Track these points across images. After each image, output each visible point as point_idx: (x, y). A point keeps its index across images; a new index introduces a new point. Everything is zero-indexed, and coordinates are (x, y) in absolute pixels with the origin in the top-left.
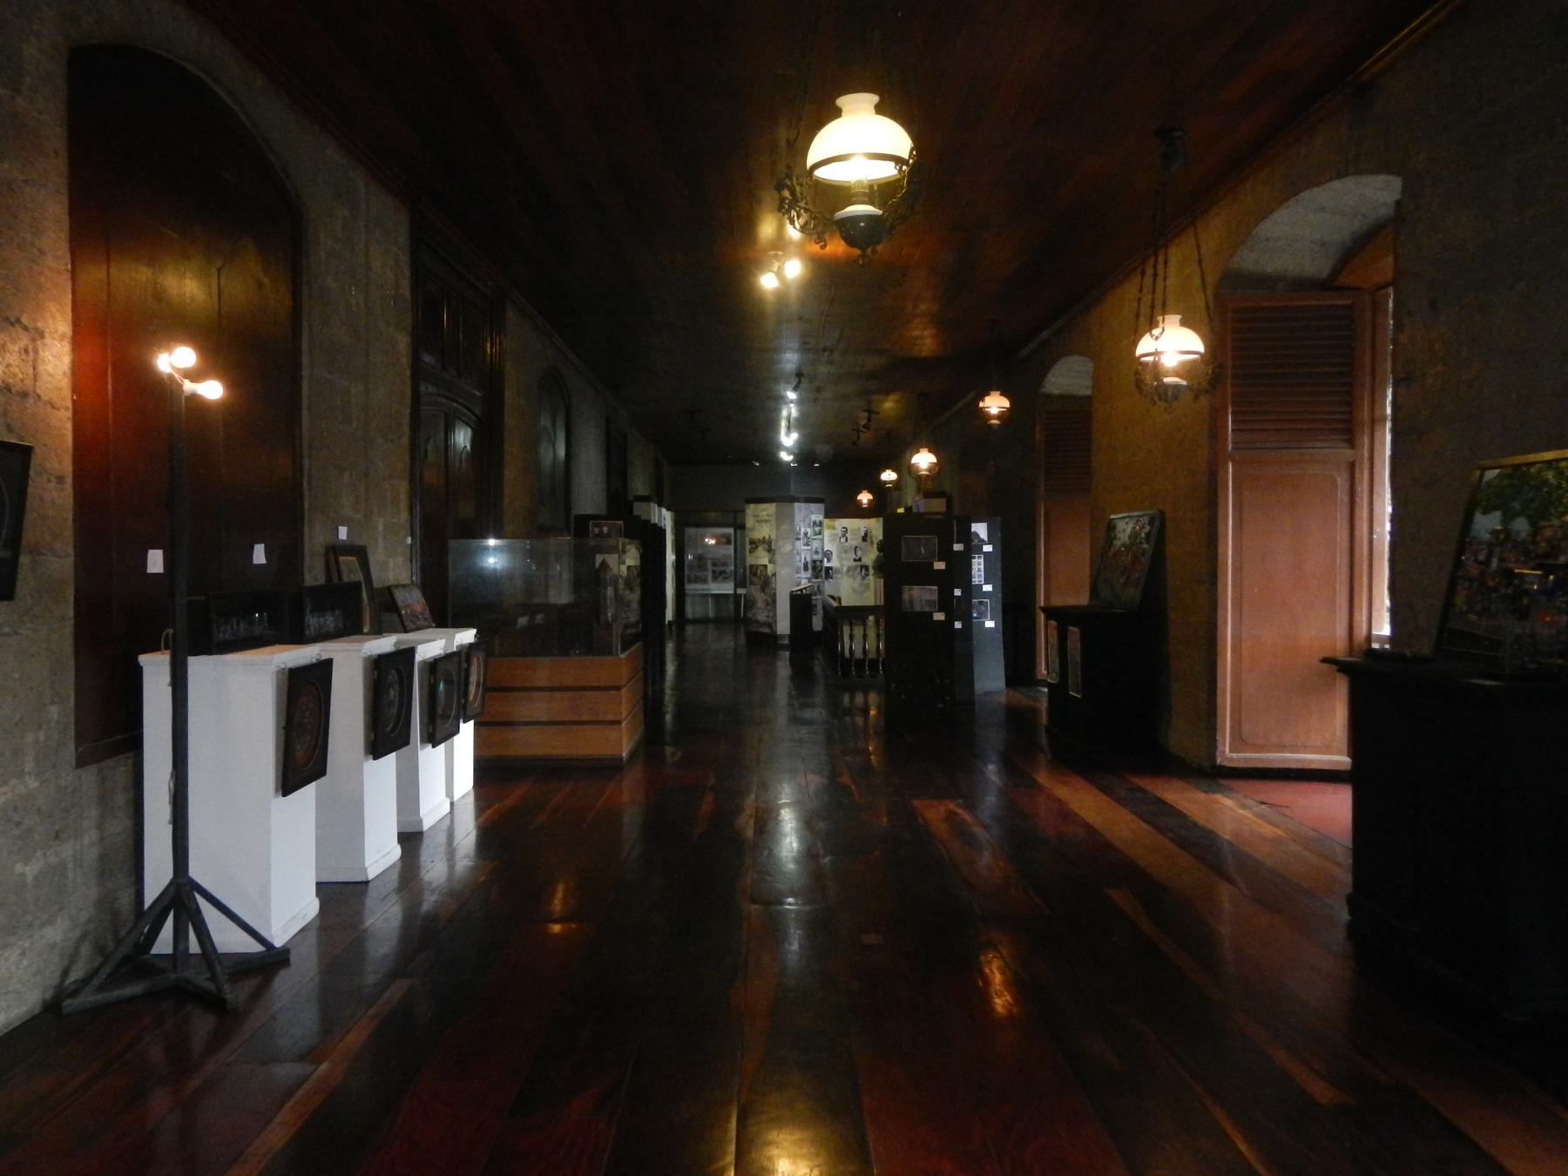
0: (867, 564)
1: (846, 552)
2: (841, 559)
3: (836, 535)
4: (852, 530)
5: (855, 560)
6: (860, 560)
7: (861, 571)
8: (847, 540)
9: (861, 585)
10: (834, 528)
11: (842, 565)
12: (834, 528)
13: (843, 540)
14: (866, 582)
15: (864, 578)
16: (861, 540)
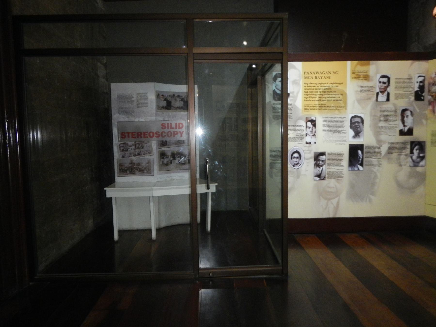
0: (421, 140)
1: (386, 119)
2: (378, 132)
3: (372, 88)
4: (398, 80)
5: (402, 133)
6: (410, 132)
7: (412, 152)
8: (388, 100)
9: (411, 175)
10: (367, 77)
11: (380, 143)
12: (367, 77)
13: (382, 98)
14: (419, 169)
15: (416, 164)
16: (413, 98)
